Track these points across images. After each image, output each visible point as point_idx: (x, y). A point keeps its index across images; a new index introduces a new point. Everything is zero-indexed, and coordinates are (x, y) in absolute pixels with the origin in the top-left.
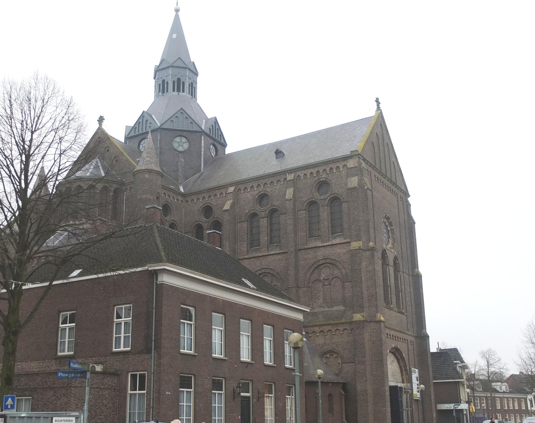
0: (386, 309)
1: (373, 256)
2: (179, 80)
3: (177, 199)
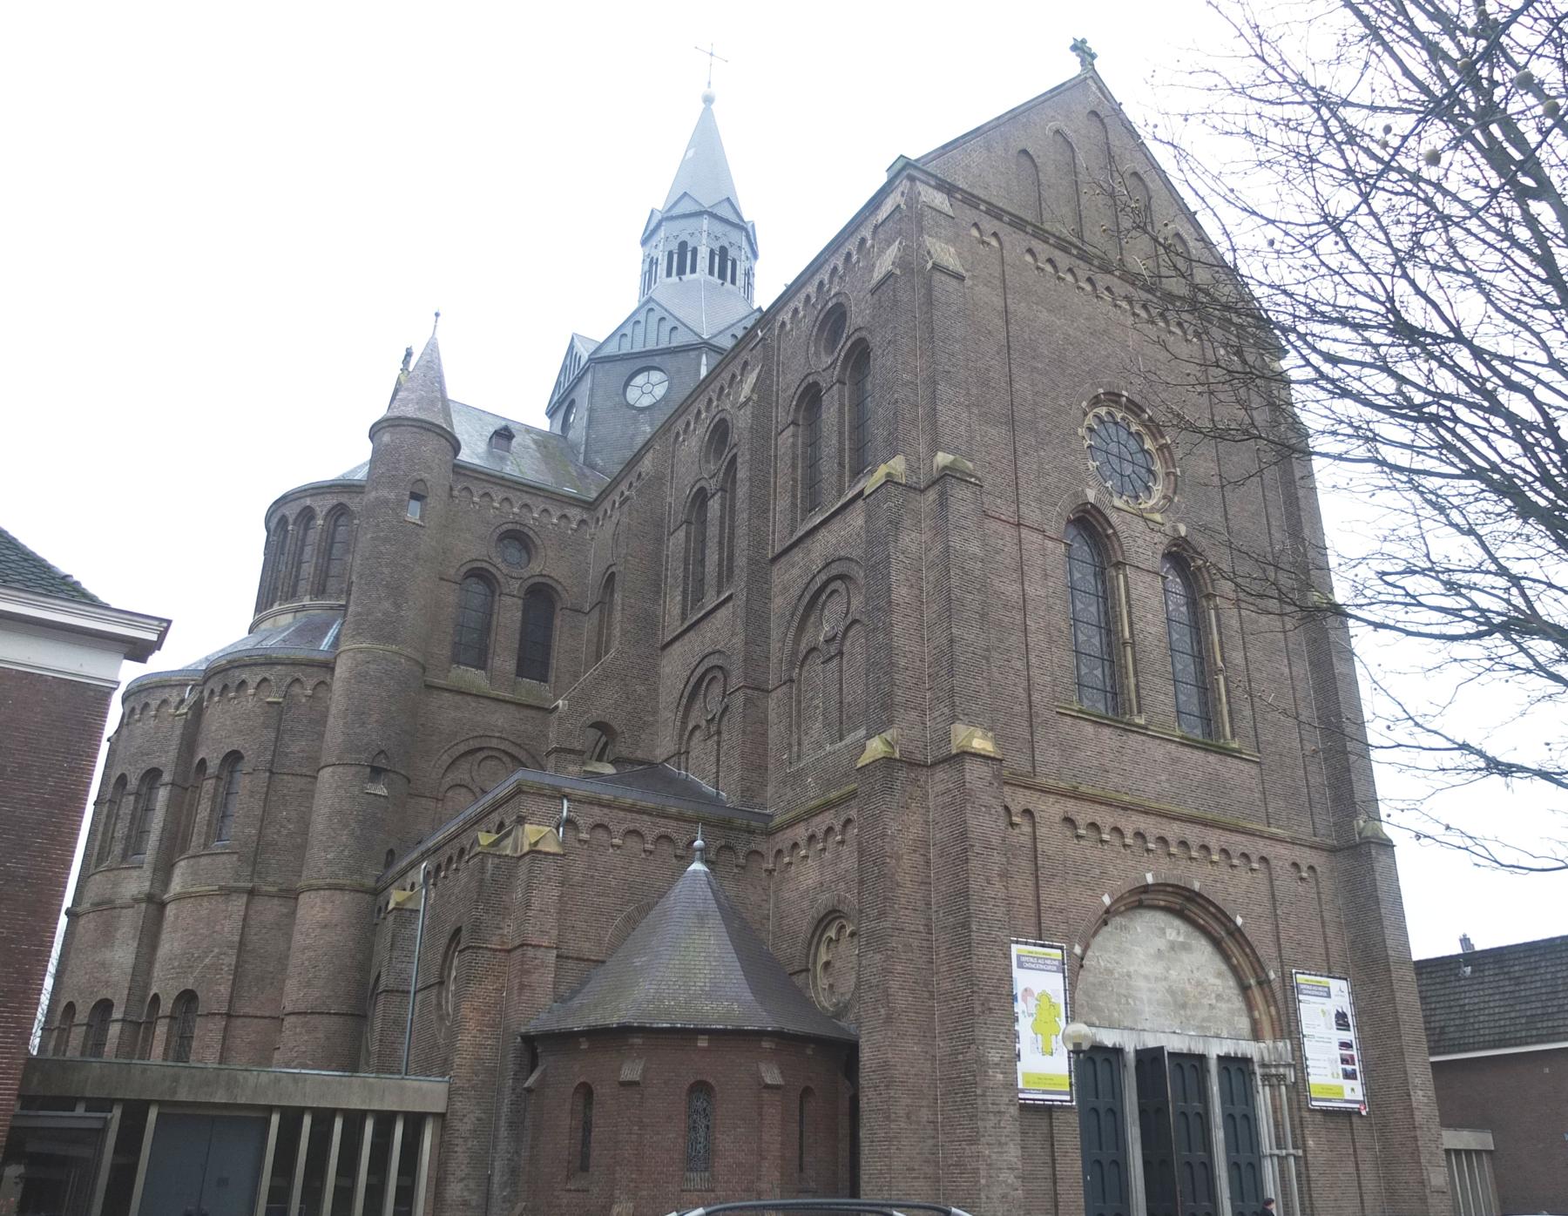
2: (683, 245)
3: (565, 516)
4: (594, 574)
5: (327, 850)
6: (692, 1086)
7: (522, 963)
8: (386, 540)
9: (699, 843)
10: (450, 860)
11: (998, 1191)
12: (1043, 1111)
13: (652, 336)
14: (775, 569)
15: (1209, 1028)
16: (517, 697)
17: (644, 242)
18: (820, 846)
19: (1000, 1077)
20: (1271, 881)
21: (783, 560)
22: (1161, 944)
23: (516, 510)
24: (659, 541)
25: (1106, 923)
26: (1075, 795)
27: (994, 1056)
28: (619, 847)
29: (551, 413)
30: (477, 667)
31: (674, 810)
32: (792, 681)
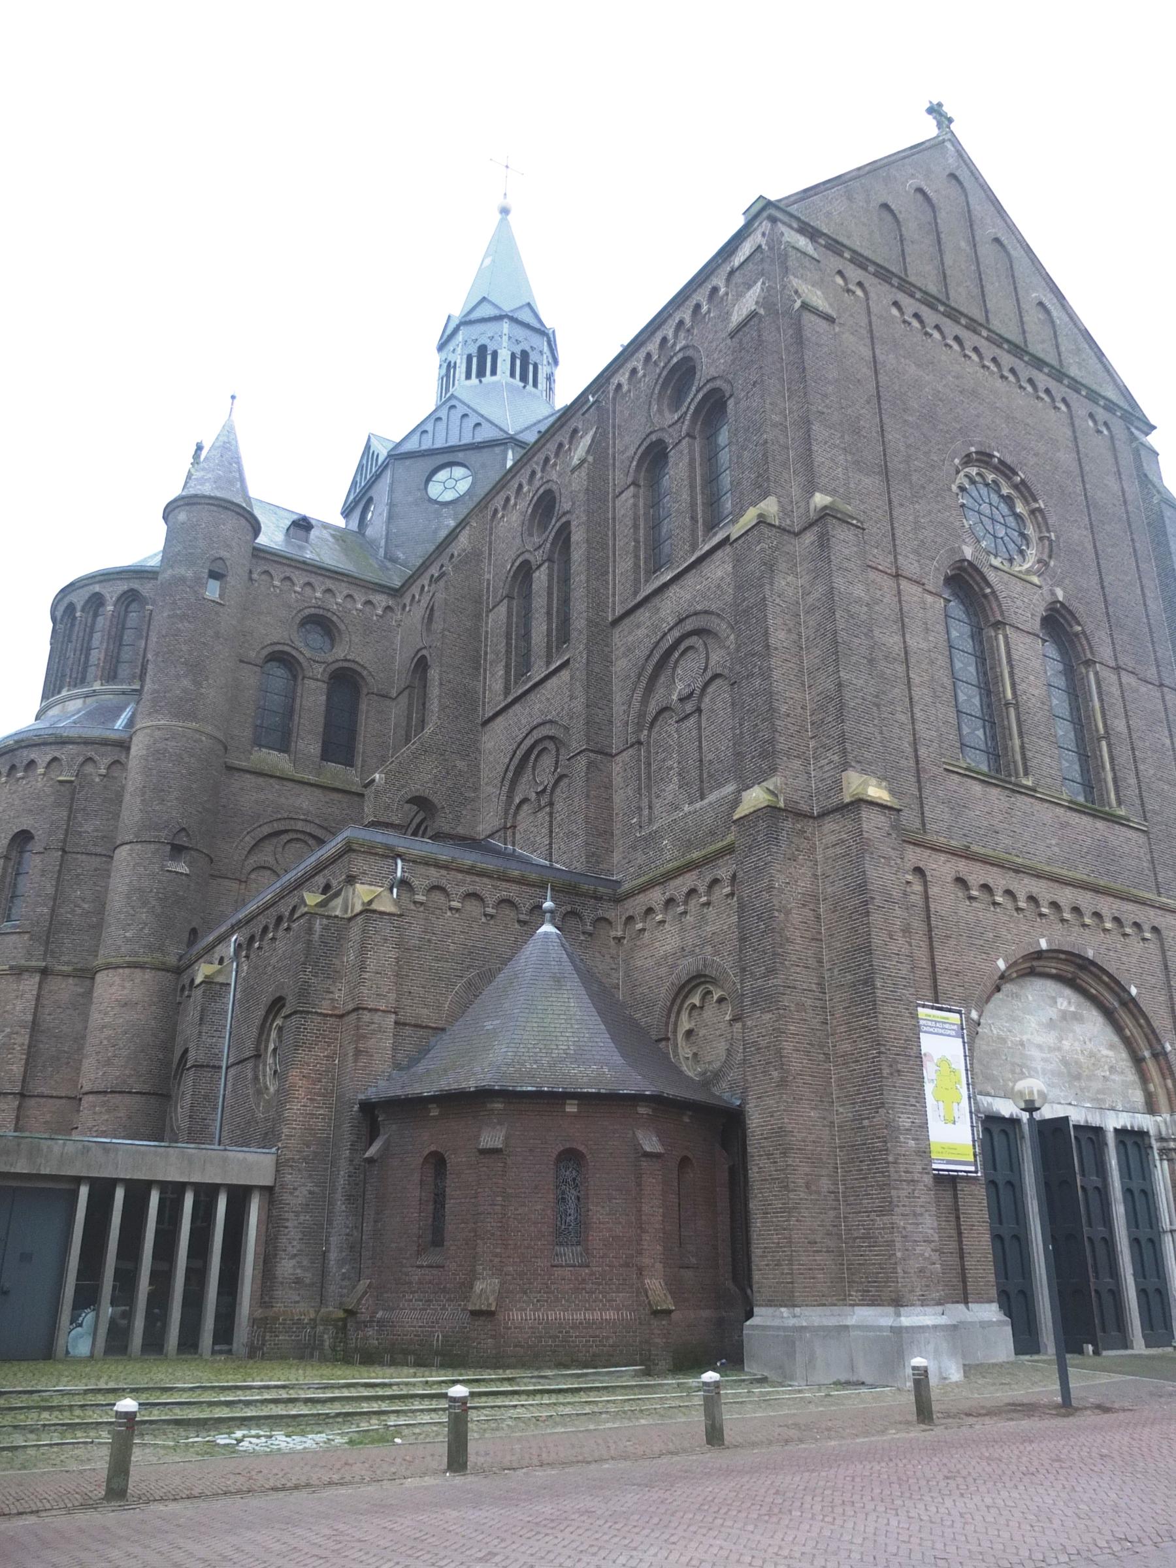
0: (977, 788)
1: (824, 542)
2: (482, 349)
3: (368, 602)
4: (402, 659)
5: (122, 933)
6: (560, 1154)
7: (358, 1028)
8: (184, 617)
9: (548, 904)
10: (265, 930)
11: (914, 1265)
12: (948, 1182)
13: (454, 432)
14: (616, 632)
15: (1103, 1100)
16: (322, 780)
17: (441, 348)
18: (681, 909)
19: (912, 1143)
20: (1163, 951)
21: (626, 621)
22: (1052, 1013)
23: (318, 595)
24: (478, 617)
25: (998, 989)
26: (966, 854)
27: (904, 1121)
28: (457, 910)
29: (347, 513)
30: (280, 751)
31: (516, 873)
32: (639, 743)
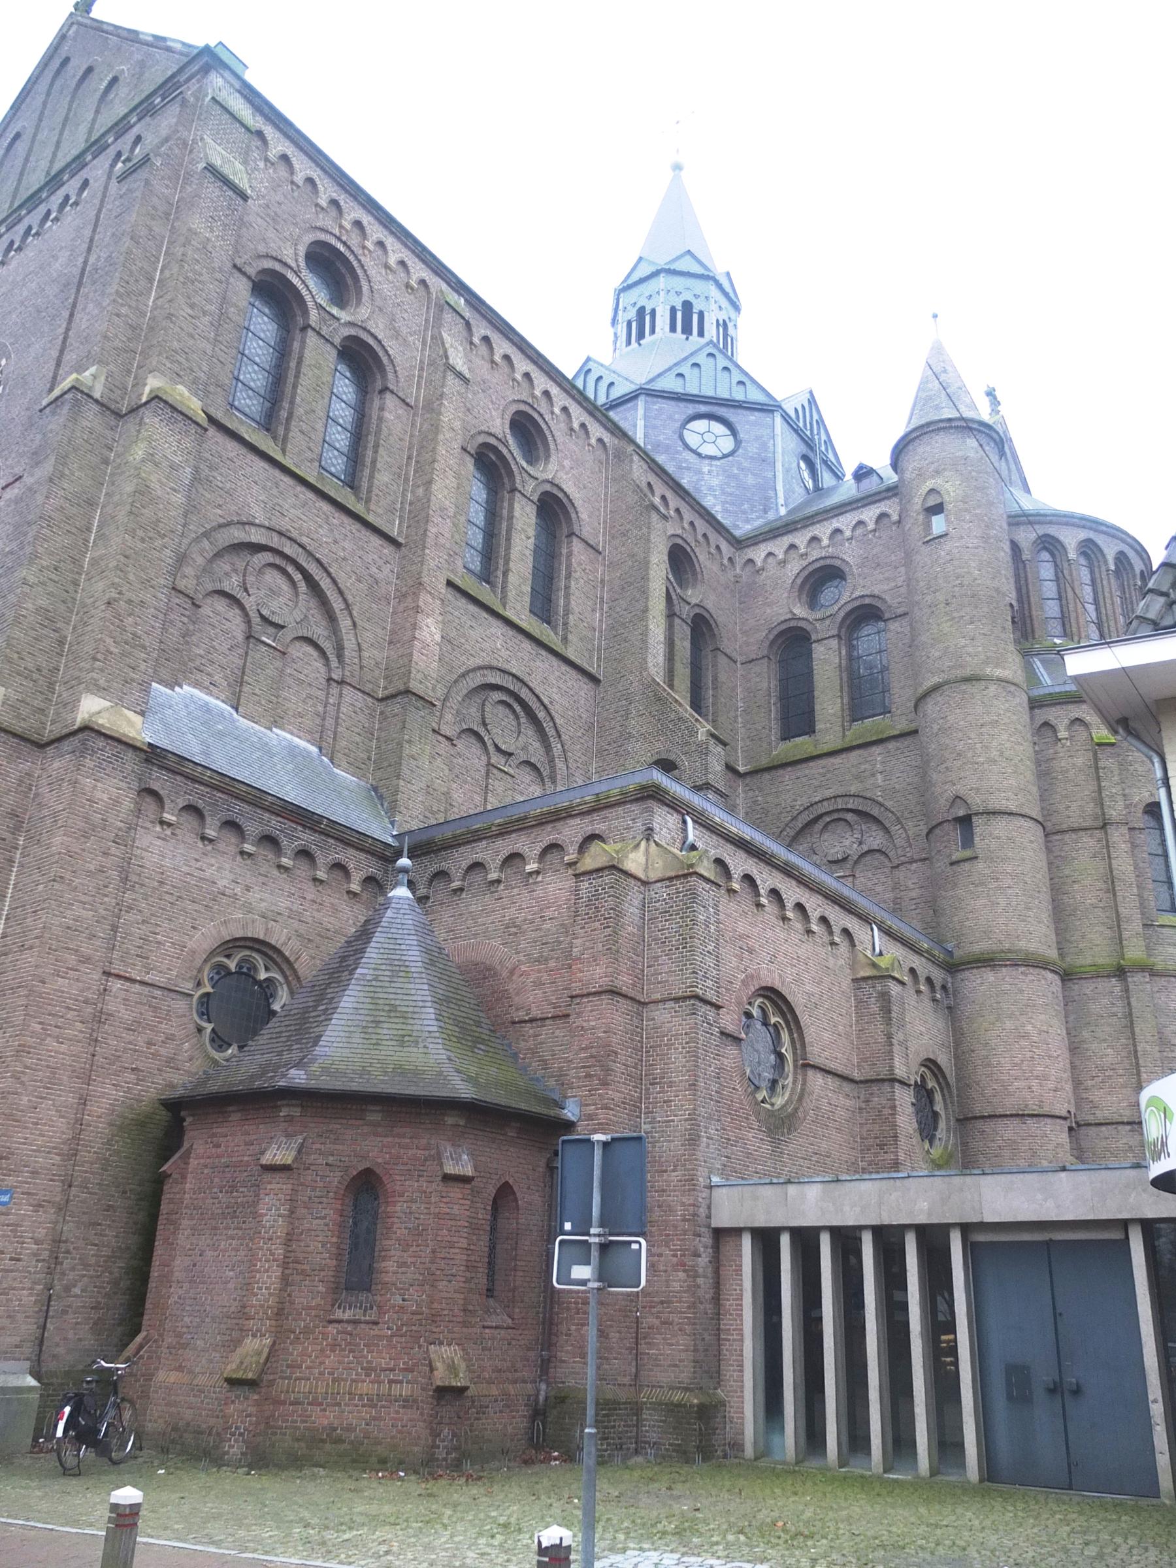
2: (641, 311)
